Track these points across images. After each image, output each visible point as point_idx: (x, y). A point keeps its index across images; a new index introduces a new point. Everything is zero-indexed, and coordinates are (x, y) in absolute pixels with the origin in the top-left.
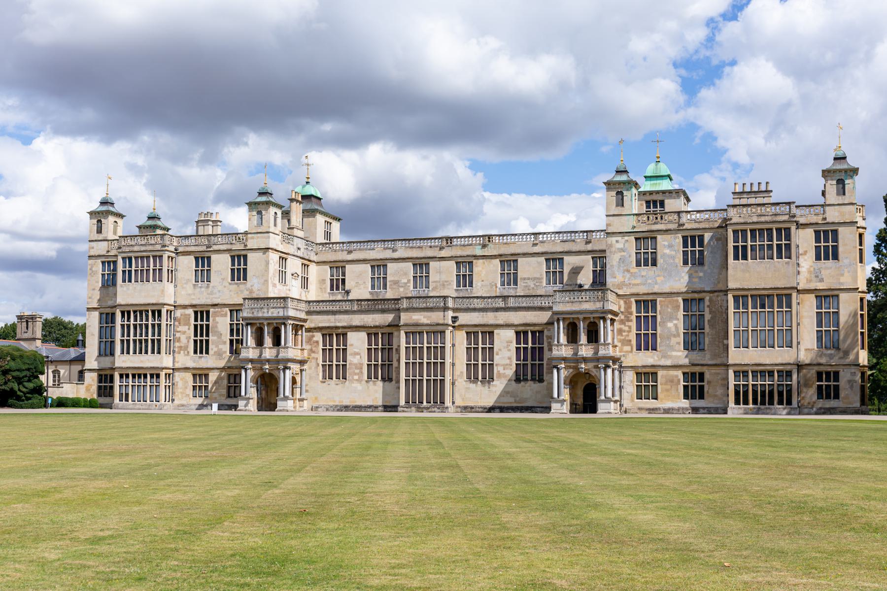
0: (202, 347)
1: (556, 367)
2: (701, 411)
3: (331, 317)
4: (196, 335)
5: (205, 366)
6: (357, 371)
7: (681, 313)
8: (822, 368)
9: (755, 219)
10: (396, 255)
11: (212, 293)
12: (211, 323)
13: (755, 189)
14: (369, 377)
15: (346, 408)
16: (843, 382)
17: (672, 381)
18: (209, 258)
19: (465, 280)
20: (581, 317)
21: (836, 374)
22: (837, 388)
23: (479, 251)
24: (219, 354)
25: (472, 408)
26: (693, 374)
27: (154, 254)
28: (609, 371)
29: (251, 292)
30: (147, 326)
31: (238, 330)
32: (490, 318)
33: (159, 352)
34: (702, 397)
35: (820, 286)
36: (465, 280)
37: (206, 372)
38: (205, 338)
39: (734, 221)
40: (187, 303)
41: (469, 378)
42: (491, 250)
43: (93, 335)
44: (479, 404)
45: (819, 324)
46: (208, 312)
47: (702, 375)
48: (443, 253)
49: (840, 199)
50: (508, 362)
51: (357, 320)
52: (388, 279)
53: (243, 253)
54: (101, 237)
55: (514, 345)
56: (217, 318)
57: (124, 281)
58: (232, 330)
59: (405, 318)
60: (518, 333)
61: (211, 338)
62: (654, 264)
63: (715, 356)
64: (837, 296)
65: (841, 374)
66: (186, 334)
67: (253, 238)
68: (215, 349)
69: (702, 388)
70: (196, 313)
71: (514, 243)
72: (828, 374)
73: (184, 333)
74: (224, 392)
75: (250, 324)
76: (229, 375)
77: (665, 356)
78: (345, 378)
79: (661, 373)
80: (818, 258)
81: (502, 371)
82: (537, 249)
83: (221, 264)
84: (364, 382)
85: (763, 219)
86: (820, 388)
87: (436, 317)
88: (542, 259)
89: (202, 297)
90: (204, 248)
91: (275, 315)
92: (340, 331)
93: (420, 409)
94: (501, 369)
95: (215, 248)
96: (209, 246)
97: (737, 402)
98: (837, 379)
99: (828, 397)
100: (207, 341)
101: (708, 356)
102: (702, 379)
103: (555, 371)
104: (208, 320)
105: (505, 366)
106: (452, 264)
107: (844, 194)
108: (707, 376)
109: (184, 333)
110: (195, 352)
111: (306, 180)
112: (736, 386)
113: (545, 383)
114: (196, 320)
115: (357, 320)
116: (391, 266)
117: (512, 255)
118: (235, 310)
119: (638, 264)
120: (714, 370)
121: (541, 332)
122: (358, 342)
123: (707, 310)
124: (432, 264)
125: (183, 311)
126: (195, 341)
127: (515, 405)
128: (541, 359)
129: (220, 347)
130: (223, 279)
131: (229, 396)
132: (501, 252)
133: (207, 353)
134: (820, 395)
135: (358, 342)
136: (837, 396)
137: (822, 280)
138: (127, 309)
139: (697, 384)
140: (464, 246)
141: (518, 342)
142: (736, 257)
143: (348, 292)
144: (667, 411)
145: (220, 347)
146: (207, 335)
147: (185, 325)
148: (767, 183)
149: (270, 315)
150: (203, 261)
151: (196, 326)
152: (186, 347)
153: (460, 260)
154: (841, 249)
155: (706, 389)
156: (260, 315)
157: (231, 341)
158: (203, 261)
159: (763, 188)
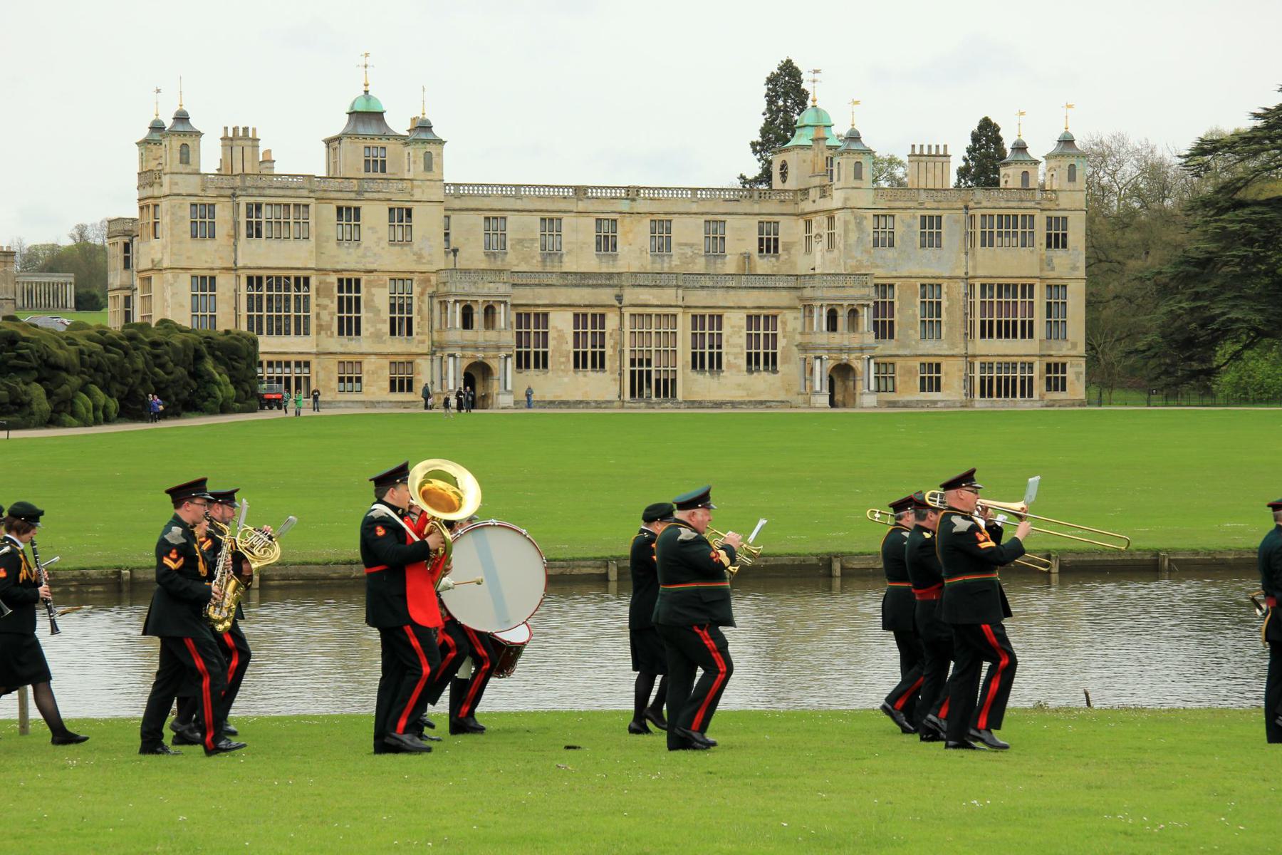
0: (349, 327)
1: (820, 358)
2: (940, 404)
3: (528, 291)
4: (340, 310)
5: (358, 350)
6: (563, 359)
7: (919, 300)
8: (1052, 360)
9: (1003, 204)
10: (519, 204)
11: (364, 256)
12: (363, 294)
13: (933, 152)
14: (576, 366)
15: (551, 402)
16: (1070, 374)
17: (909, 371)
18: (357, 210)
19: (606, 244)
20: (846, 303)
21: (1064, 365)
22: (1064, 379)
23: (625, 206)
24: (377, 336)
25: (700, 402)
26: (931, 364)
27: (298, 201)
28: (872, 362)
29: (420, 257)
30: (287, 299)
31: (401, 306)
32: (719, 298)
33: (307, 333)
34: (938, 389)
35: (1052, 274)
36: (606, 244)
37: (358, 358)
38: (354, 315)
39: (985, 204)
40: (328, 267)
41: (694, 366)
42: (640, 206)
43: (181, 306)
44: (708, 399)
45: (1049, 315)
46: (358, 281)
47: (938, 365)
48: (581, 206)
49: (1071, 186)
50: (738, 350)
51: (563, 296)
52: (508, 237)
53: (408, 205)
54: (189, 169)
55: (744, 332)
56: (374, 290)
57: (249, 236)
58: (392, 306)
59: (630, 296)
60: (749, 317)
61: (364, 314)
62: (892, 245)
63: (953, 345)
64: (1065, 286)
65: (1068, 366)
66: (324, 309)
67: (419, 187)
68: (372, 330)
69: (938, 379)
70: (340, 281)
71: (667, 199)
72: (1056, 365)
73: (325, 307)
74: (387, 384)
75: (459, 301)
76: (391, 363)
77: (904, 346)
78: (545, 365)
79: (899, 363)
80: (1049, 245)
81: (731, 358)
82: (694, 208)
83: (374, 215)
84: (571, 373)
85: (1011, 204)
86: (1049, 379)
87: (668, 296)
88: (701, 220)
89: (349, 259)
90: (353, 195)
91: (493, 292)
92: (540, 310)
93: (650, 405)
94: (731, 358)
95: (367, 195)
96: (358, 193)
97: (982, 395)
98: (1064, 371)
99: (1056, 389)
100: (358, 320)
101: (945, 346)
102: (938, 371)
103: (818, 362)
104: (358, 291)
105: (736, 356)
106: (591, 221)
107: (1074, 180)
108: (943, 368)
109: (325, 307)
110: (341, 333)
111: (364, 88)
112: (982, 381)
113: (779, 374)
114: (340, 290)
115: (563, 296)
116: (512, 219)
117: (666, 214)
118: (400, 280)
119: (876, 245)
120: (951, 361)
121: (775, 317)
122: (561, 323)
123: (944, 296)
124: (567, 220)
125: (323, 277)
126: (340, 319)
127: (747, 399)
128: (775, 347)
129: (379, 326)
130: (380, 239)
131: (393, 389)
132: (651, 210)
133: (358, 333)
134: (1049, 389)
135: (561, 323)
136: (1064, 389)
137: (1053, 269)
138: (259, 273)
139: (934, 375)
140: (606, 198)
141: (749, 328)
142: (983, 245)
143: (455, 251)
144: (906, 405)
145: (379, 326)
146: (358, 310)
147: (326, 296)
148: (945, 146)
149: (486, 291)
150: (349, 214)
151: (341, 299)
152: (329, 327)
153: (602, 216)
154: (1070, 239)
155: (943, 381)
156: (473, 290)
157: (393, 320)
158: (349, 214)
159: (941, 152)
